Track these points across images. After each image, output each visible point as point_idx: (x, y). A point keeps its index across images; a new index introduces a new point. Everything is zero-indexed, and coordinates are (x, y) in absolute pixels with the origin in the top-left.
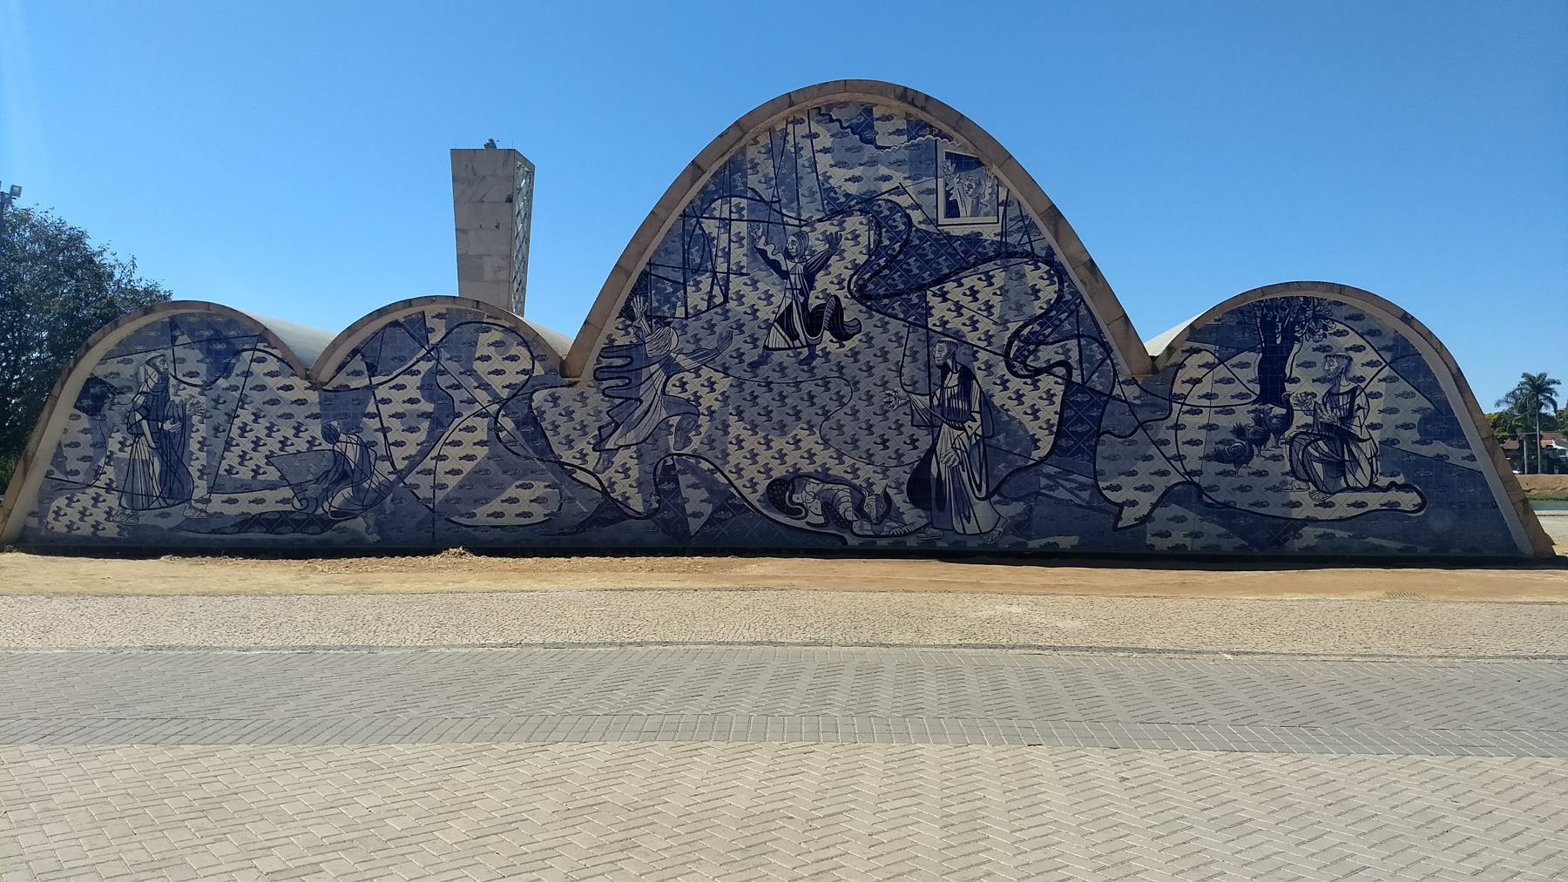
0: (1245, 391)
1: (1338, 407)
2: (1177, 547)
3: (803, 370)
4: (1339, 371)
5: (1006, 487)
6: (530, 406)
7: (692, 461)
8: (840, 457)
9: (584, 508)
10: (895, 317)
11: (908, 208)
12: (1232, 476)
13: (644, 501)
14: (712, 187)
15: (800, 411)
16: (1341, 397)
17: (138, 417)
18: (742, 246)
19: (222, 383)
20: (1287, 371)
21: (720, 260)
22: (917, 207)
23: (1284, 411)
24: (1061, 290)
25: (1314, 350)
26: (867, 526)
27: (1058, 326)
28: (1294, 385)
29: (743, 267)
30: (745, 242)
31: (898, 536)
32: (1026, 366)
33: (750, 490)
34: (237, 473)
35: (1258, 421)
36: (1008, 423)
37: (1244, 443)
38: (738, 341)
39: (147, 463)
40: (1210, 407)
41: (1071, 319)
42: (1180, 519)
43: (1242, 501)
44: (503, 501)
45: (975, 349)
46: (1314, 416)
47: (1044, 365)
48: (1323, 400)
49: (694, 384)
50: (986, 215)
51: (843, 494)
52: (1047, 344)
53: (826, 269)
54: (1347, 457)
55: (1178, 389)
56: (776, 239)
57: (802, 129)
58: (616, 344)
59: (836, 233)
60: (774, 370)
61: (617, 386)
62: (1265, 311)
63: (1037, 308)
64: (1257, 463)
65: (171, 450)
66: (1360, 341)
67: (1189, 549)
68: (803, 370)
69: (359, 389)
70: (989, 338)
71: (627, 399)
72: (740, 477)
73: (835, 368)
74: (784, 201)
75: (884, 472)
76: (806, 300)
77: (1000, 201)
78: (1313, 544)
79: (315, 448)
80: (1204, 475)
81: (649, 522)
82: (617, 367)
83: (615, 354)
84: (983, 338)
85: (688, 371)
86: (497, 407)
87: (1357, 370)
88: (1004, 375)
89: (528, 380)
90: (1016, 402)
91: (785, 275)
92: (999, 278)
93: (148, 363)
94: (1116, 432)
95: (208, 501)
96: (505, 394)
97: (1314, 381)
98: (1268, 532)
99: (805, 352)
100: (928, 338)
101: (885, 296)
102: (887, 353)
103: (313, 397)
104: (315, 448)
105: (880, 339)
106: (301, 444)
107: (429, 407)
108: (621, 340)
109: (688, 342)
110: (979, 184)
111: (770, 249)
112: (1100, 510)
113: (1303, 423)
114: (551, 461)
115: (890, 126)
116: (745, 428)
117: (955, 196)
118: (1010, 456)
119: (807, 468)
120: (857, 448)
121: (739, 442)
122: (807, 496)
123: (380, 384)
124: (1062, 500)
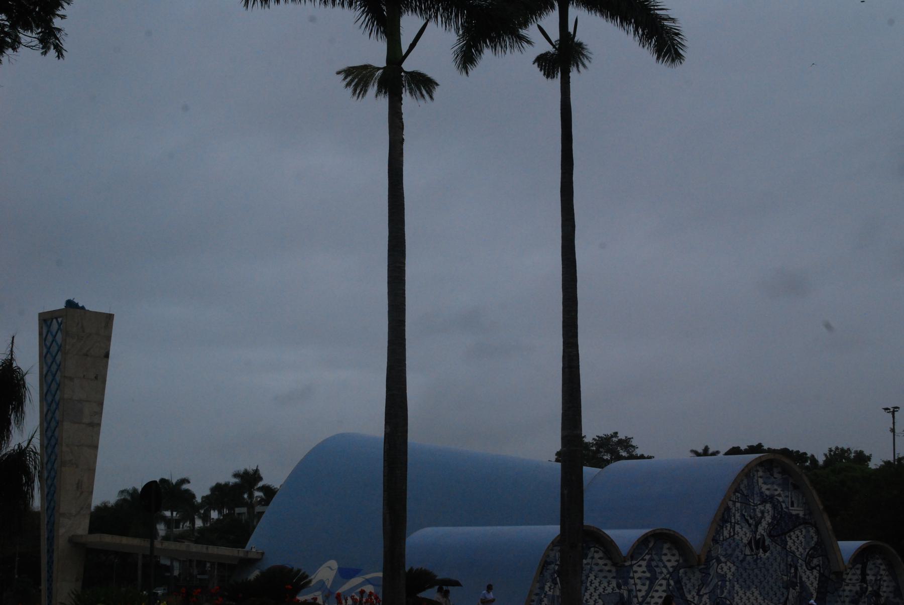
7: (724, 600)
10: (779, 545)
17: (556, 576)
18: (738, 513)
21: (733, 517)
22: (784, 502)
24: (818, 538)
30: (739, 511)
32: (810, 566)
34: (589, 602)
38: (737, 552)
49: (725, 569)
52: (816, 558)
63: (812, 544)
70: (801, 554)
74: (750, 496)
76: (756, 536)
79: (614, 592)
86: (668, 576)
89: (678, 564)
91: (750, 525)
92: (804, 531)
96: (671, 570)
103: (614, 569)
104: (614, 592)
106: (609, 590)
107: (648, 575)
111: (746, 514)
117: (793, 499)
121: (737, 593)
123: (635, 564)
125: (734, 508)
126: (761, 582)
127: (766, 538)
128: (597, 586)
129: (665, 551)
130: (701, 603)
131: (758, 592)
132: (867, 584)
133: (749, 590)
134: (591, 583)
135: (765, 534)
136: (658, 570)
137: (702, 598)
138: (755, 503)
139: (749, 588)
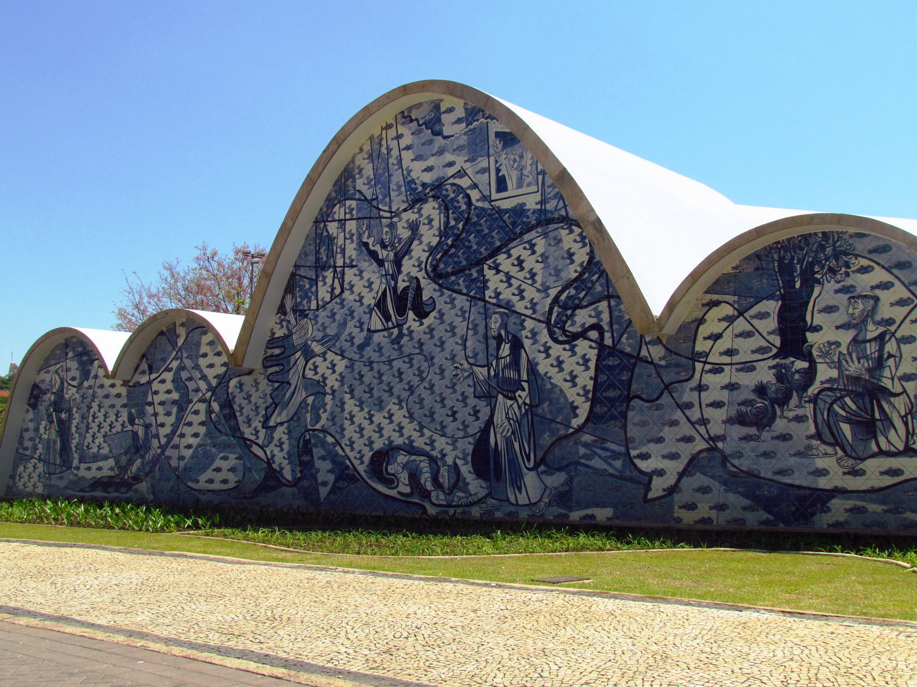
0: (765, 344)
1: (866, 358)
2: (703, 521)
3: (394, 349)
4: (865, 314)
5: (550, 457)
6: (228, 392)
7: (322, 435)
8: (421, 427)
9: (258, 477)
10: (460, 292)
11: (469, 188)
12: (755, 441)
13: (293, 471)
14: (334, 194)
15: (392, 388)
16: (868, 345)
17: (52, 410)
18: (353, 242)
19: (86, 384)
20: (808, 319)
21: (339, 256)
22: (475, 186)
23: (805, 365)
25: (837, 292)
26: (442, 497)
27: (590, 288)
28: (816, 333)
29: (353, 260)
30: (355, 238)
31: (465, 506)
32: (564, 332)
33: (359, 462)
35: (780, 378)
36: (551, 391)
37: (766, 403)
38: (351, 327)
39: (55, 442)
40: (731, 364)
41: (602, 280)
42: (705, 490)
43: (766, 469)
44: (214, 470)
45: (523, 317)
46: (839, 367)
47: (580, 330)
48: (848, 349)
50: (529, 185)
51: (424, 465)
52: (582, 307)
53: (410, 253)
54: (877, 416)
55: (701, 346)
56: (375, 232)
57: (392, 133)
58: (276, 336)
59: (416, 219)
60: (374, 351)
61: (276, 372)
62: (782, 252)
63: (571, 272)
64: (780, 425)
66: (885, 277)
67: (715, 523)
68: (394, 349)
69: (143, 384)
70: (533, 305)
71: (283, 383)
72: (352, 449)
73: (417, 345)
74: (380, 197)
75: (453, 444)
76: (396, 284)
77: (539, 170)
78: (842, 519)
79: (125, 429)
80: (728, 439)
81: (295, 490)
82: (277, 356)
83: (275, 345)
84: (529, 306)
85: (319, 356)
86: (209, 394)
87: (885, 311)
88: (546, 342)
89: (226, 371)
90: (557, 369)
91: (381, 263)
92: (541, 245)
93: (56, 372)
94: (644, 396)
95: (78, 468)
96: (214, 382)
97: (837, 328)
98: (794, 505)
99: (396, 331)
100: (486, 309)
101: (453, 274)
102: (454, 327)
103: (124, 391)
104: (125, 429)
105: (451, 315)
106: (118, 428)
108: (279, 333)
109: (319, 330)
110: (521, 157)
111: (371, 241)
112: (631, 480)
113: (827, 377)
114: (238, 437)
115: (452, 117)
116: (355, 405)
118: (553, 425)
119: (398, 441)
120: (433, 420)
121: (352, 417)
122: (397, 466)
124: (598, 470)
125: (341, 236)
126: (411, 389)
127: (423, 283)
128: (102, 421)
129: (204, 349)
130: (270, 443)
131: (404, 412)
132: (809, 357)
133: (381, 409)
134: (94, 417)
135: (421, 275)
136: (191, 385)
137: (273, 432)
138: (393, 210)
139: (380, 405)
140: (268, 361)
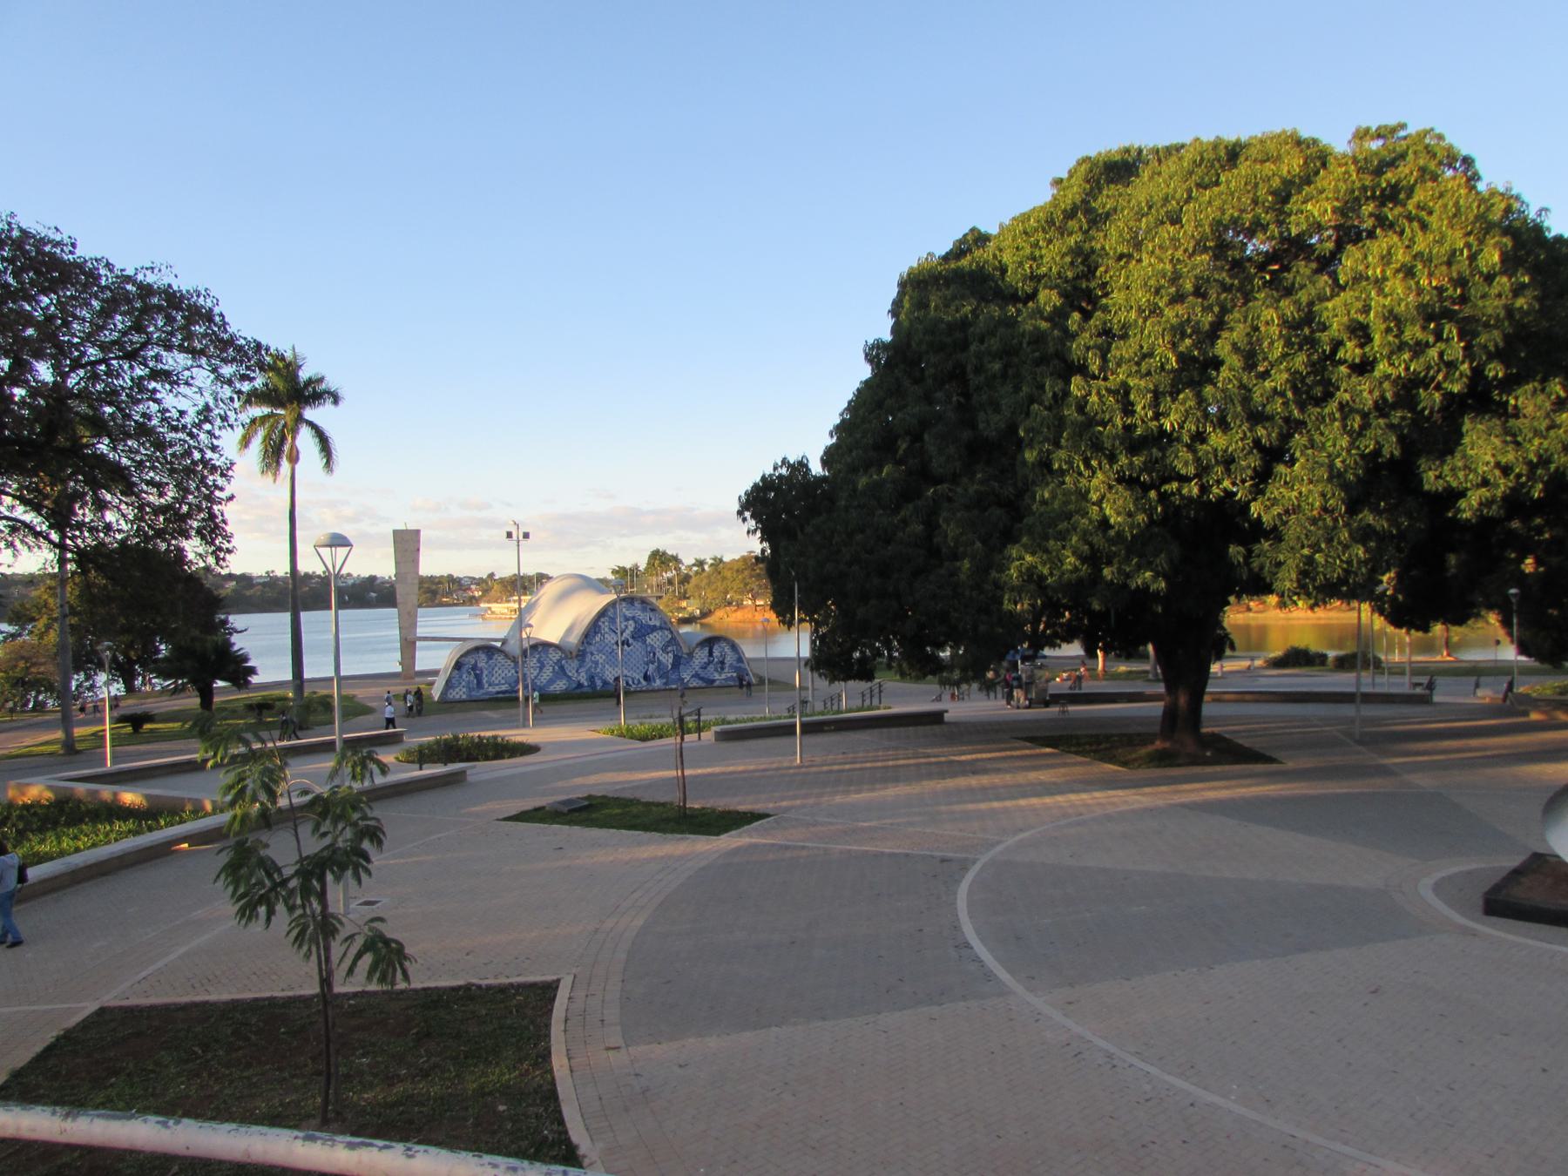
9: (574, 685)
38: (607, 648)
63: (667, 640)
65: (478, 678)
140: (577, 656)
